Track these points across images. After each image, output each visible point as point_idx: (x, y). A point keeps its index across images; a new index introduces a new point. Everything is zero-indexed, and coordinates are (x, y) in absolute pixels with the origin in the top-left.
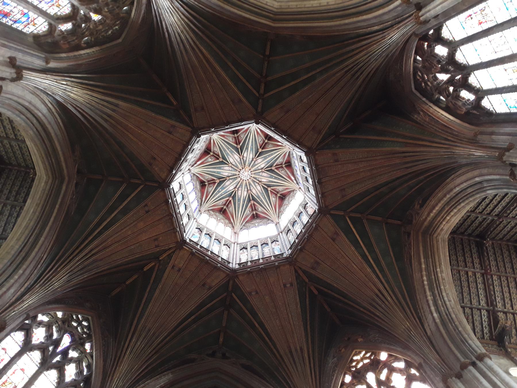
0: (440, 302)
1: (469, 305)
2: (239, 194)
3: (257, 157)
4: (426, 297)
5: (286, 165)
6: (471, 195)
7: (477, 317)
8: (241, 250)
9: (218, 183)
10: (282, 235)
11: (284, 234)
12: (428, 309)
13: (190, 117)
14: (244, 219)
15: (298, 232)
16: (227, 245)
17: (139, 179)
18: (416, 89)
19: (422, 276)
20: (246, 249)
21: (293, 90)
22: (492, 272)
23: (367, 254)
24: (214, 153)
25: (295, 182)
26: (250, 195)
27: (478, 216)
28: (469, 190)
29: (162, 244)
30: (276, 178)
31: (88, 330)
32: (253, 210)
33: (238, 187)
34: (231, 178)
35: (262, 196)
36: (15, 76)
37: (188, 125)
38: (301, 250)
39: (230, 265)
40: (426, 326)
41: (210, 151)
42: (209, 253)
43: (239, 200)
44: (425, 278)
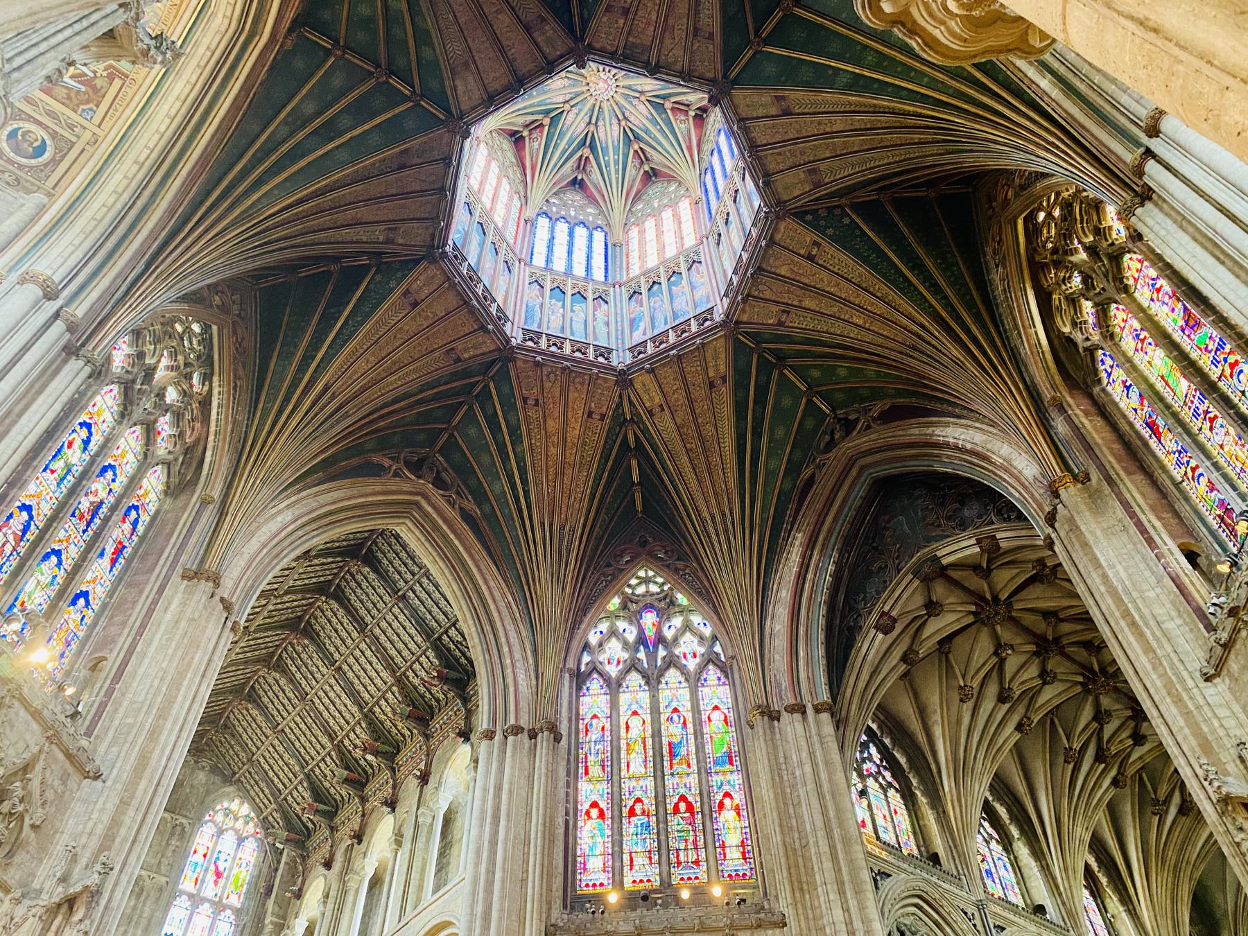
2: (637, 122)
14: (690, 149)
29: (604, 409)
33: (621, 117)
38: (766, 184)
41: (517, 132)
43: (647, 131)
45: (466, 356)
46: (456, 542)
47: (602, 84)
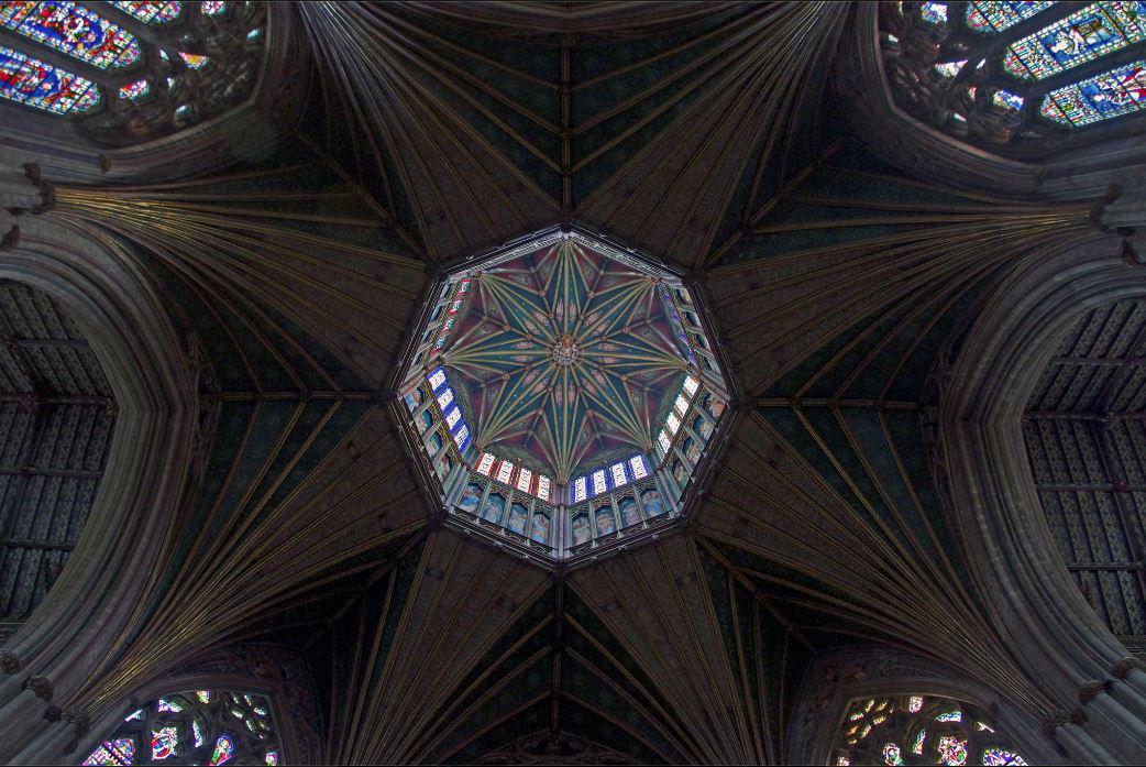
0: (1020, 564)
1: (1088, 564)
2: (559, 399)
3: (587, 311)
4: (988, 557)
5: (654, 319)
6: (1053, 315)
7: (1109, 588)
8: (574, 519)
9: (509, 382)
10: (664, 474)
11: (668, 473)
12: (996, 585)
13: (419, 240)
15: (696, 460)
16: (542, 513)
17: (331, 389)
18: (898, 105)
19: (975, 515)
20: (586, 515)
21: (636, 143)
22: (1132, 485)
23: (851, 484)
24: (490, 316)
25: (678, 353)
26: (584, 399)
27: (1081, 364)
28: (1044, 306)
30: (635, 352)
31: (267, 724)
32: (593, 431)
33: (553, 384)
34: (534, 365)
35: (611, 398)
36: (39, 200)
37: (417, 258)
39: (553, 554)
40: (996, 621)
42: (502, 533)
44: (981, 517)
45: (357, 358)
46: (165, 477)
47: (568, 350)
